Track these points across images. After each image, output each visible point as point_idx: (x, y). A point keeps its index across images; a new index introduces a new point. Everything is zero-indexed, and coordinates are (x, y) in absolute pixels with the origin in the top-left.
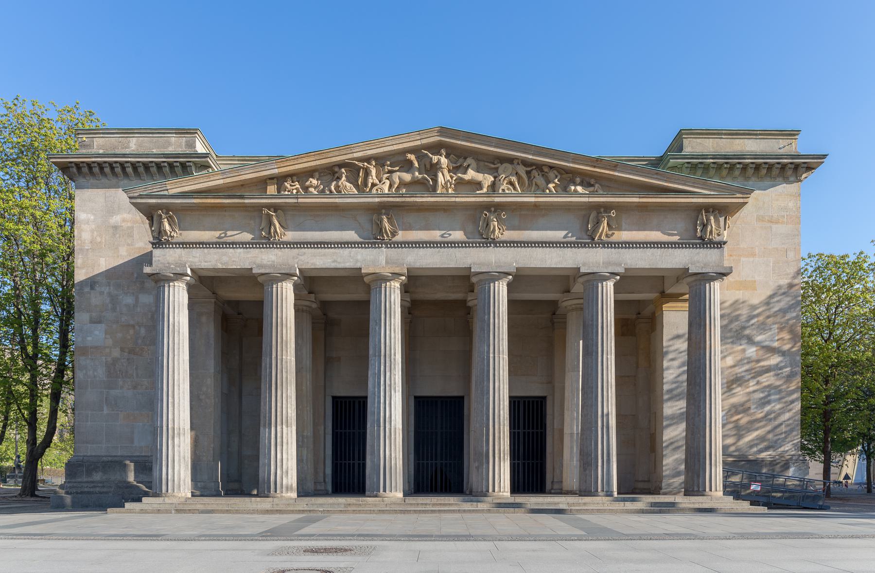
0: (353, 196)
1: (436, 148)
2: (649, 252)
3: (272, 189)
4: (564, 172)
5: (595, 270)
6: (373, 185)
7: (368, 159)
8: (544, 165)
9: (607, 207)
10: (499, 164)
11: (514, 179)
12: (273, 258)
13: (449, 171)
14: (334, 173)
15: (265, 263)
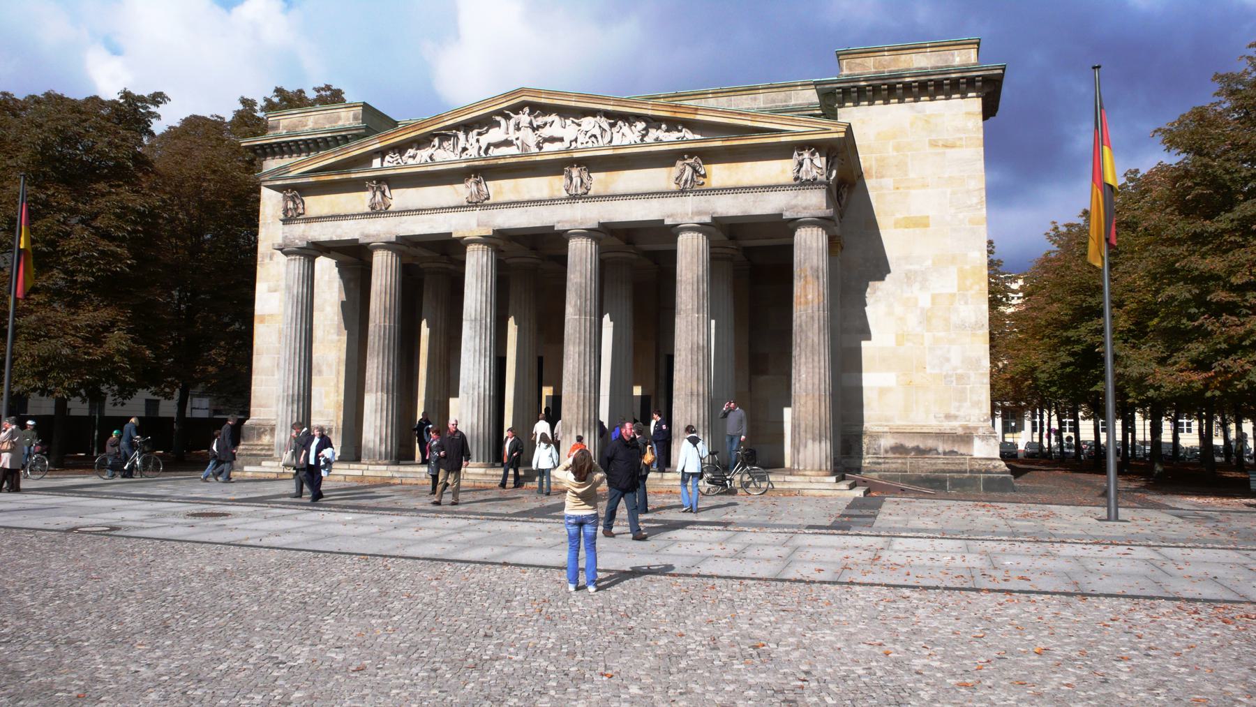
2: (742, 197)
3: (376, 163)
4: (650, 120)
5: (678, 221)
6: (465, 149)
7: (457, 127)
9: (691, 153)
11: (597, 131)
13: (534, 129)
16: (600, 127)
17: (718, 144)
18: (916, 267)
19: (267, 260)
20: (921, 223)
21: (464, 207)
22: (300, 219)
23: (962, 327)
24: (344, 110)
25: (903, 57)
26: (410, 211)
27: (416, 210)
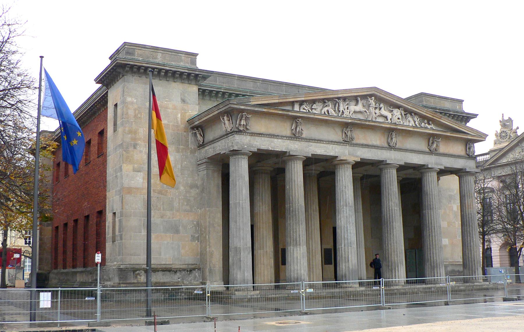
0: (334, 117)
1: (371, 96)
3: (297, 108)
8: (412, 112)
10: (393, 109)
11: (400, 116)
12: (297, 146)
14: (325, 102)
15: (293, 149)
16: (401, 114)
17: (449, 134)
18: (452, 193)
19: (131, 149)
21: (342, 143)
22: (248, 133)
24: (184, 55)
25: (442, 102)
26: (316, 140)
27: (318, 140)
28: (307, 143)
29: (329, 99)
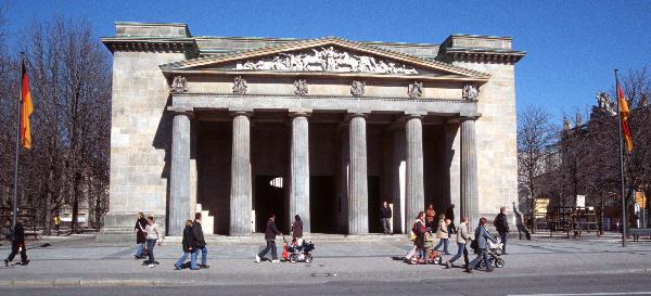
1: (327, 47)
9: (419, 81)
19: (119, 114)
20: (489, 119)
23: (508, 167)
28: (252, 99)
29: (277, 54)
